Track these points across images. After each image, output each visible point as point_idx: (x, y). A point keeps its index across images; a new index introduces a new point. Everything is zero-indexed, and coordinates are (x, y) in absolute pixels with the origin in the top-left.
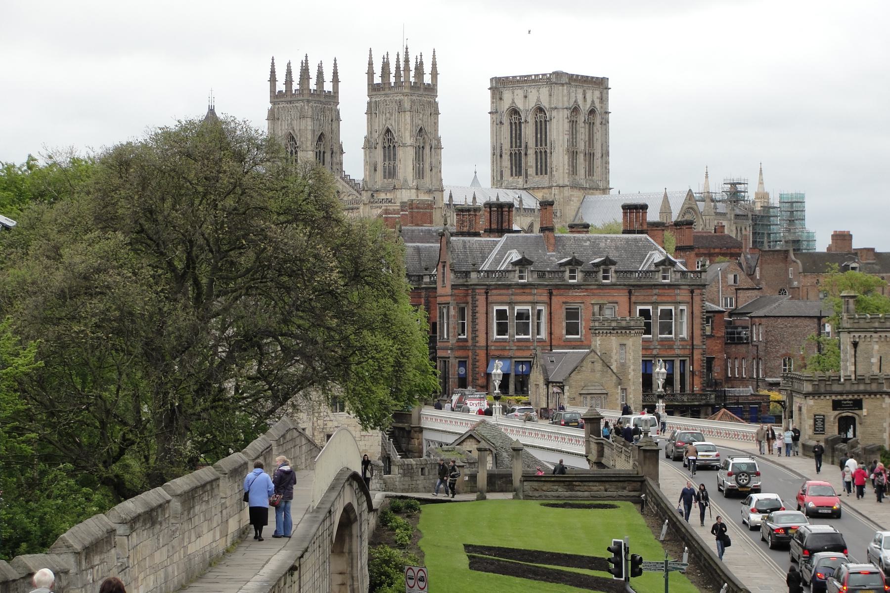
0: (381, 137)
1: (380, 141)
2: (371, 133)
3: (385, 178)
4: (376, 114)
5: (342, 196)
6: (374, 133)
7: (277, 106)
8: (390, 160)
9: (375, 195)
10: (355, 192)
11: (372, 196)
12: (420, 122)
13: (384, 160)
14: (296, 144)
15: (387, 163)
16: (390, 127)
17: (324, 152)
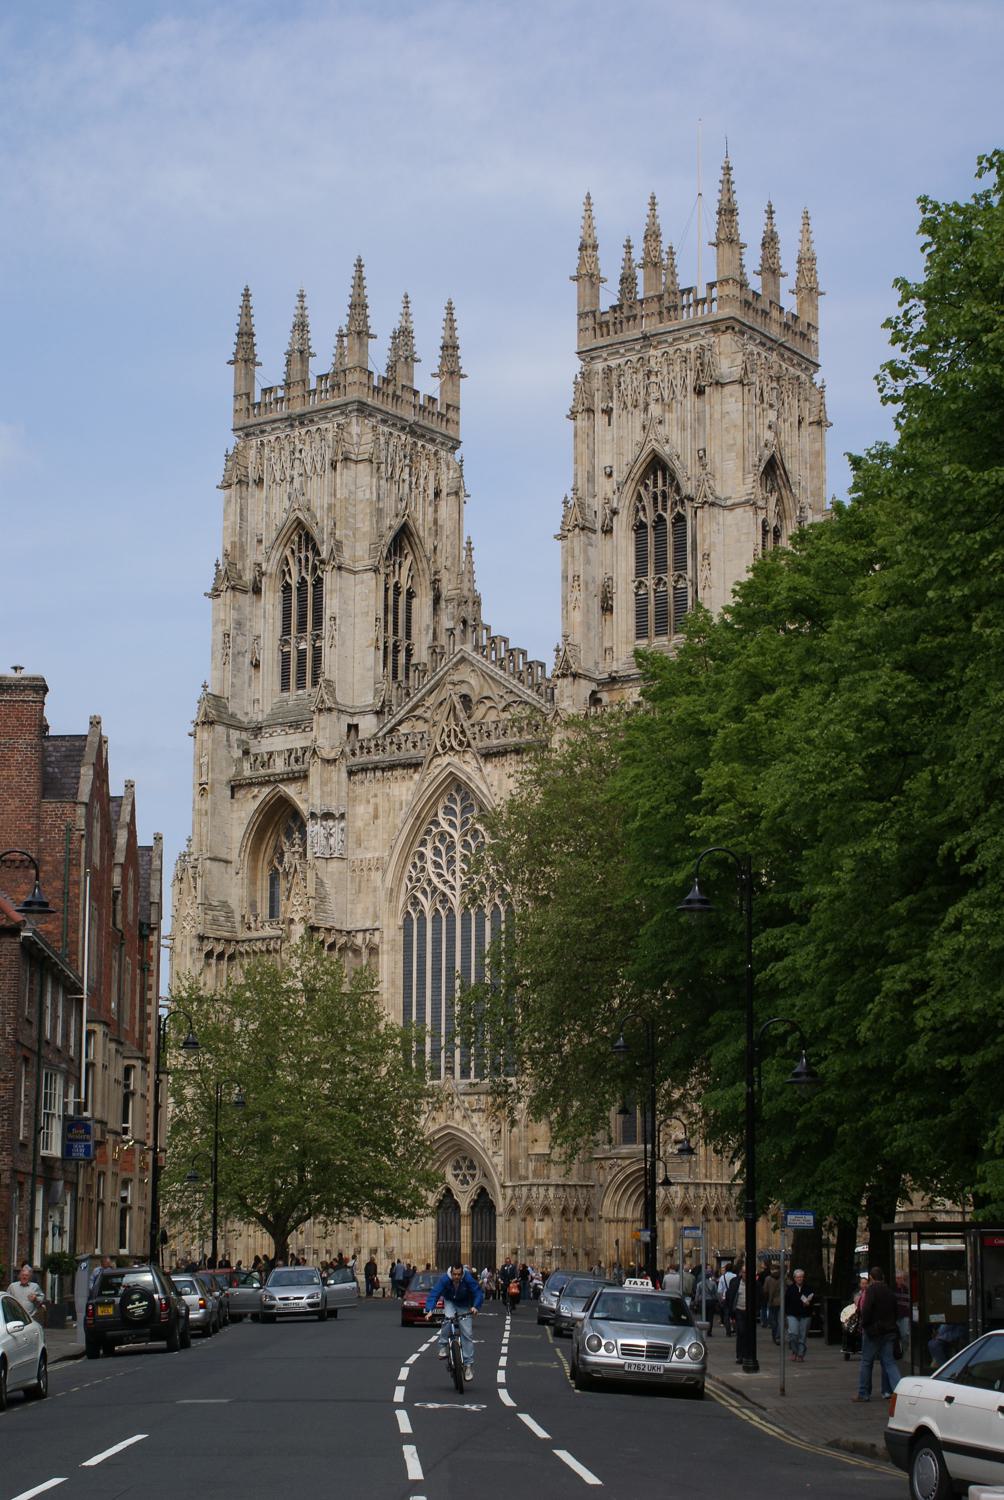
0: (629, 489)
1: (625, 505)
2: (591, 479)
3: (641, 632)
4: (608, 412)
5: (479, 712)
6: (601, 478)
7: (254, 442)
8: (661, 566)
9: (605, 697)
10: (529, 694)
11: (595, 700)
12: (769, 435)
13: (641, 570)
14: (317, 553)
15: (650, 581)
16: (665, 451)
17: (411, 595)
